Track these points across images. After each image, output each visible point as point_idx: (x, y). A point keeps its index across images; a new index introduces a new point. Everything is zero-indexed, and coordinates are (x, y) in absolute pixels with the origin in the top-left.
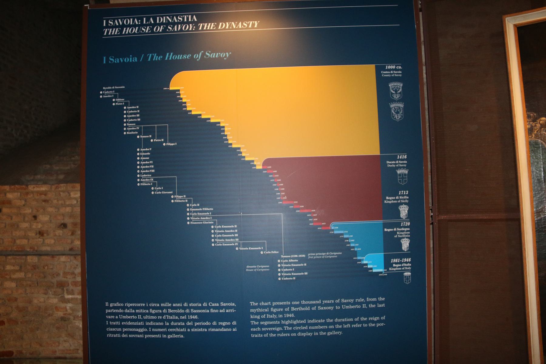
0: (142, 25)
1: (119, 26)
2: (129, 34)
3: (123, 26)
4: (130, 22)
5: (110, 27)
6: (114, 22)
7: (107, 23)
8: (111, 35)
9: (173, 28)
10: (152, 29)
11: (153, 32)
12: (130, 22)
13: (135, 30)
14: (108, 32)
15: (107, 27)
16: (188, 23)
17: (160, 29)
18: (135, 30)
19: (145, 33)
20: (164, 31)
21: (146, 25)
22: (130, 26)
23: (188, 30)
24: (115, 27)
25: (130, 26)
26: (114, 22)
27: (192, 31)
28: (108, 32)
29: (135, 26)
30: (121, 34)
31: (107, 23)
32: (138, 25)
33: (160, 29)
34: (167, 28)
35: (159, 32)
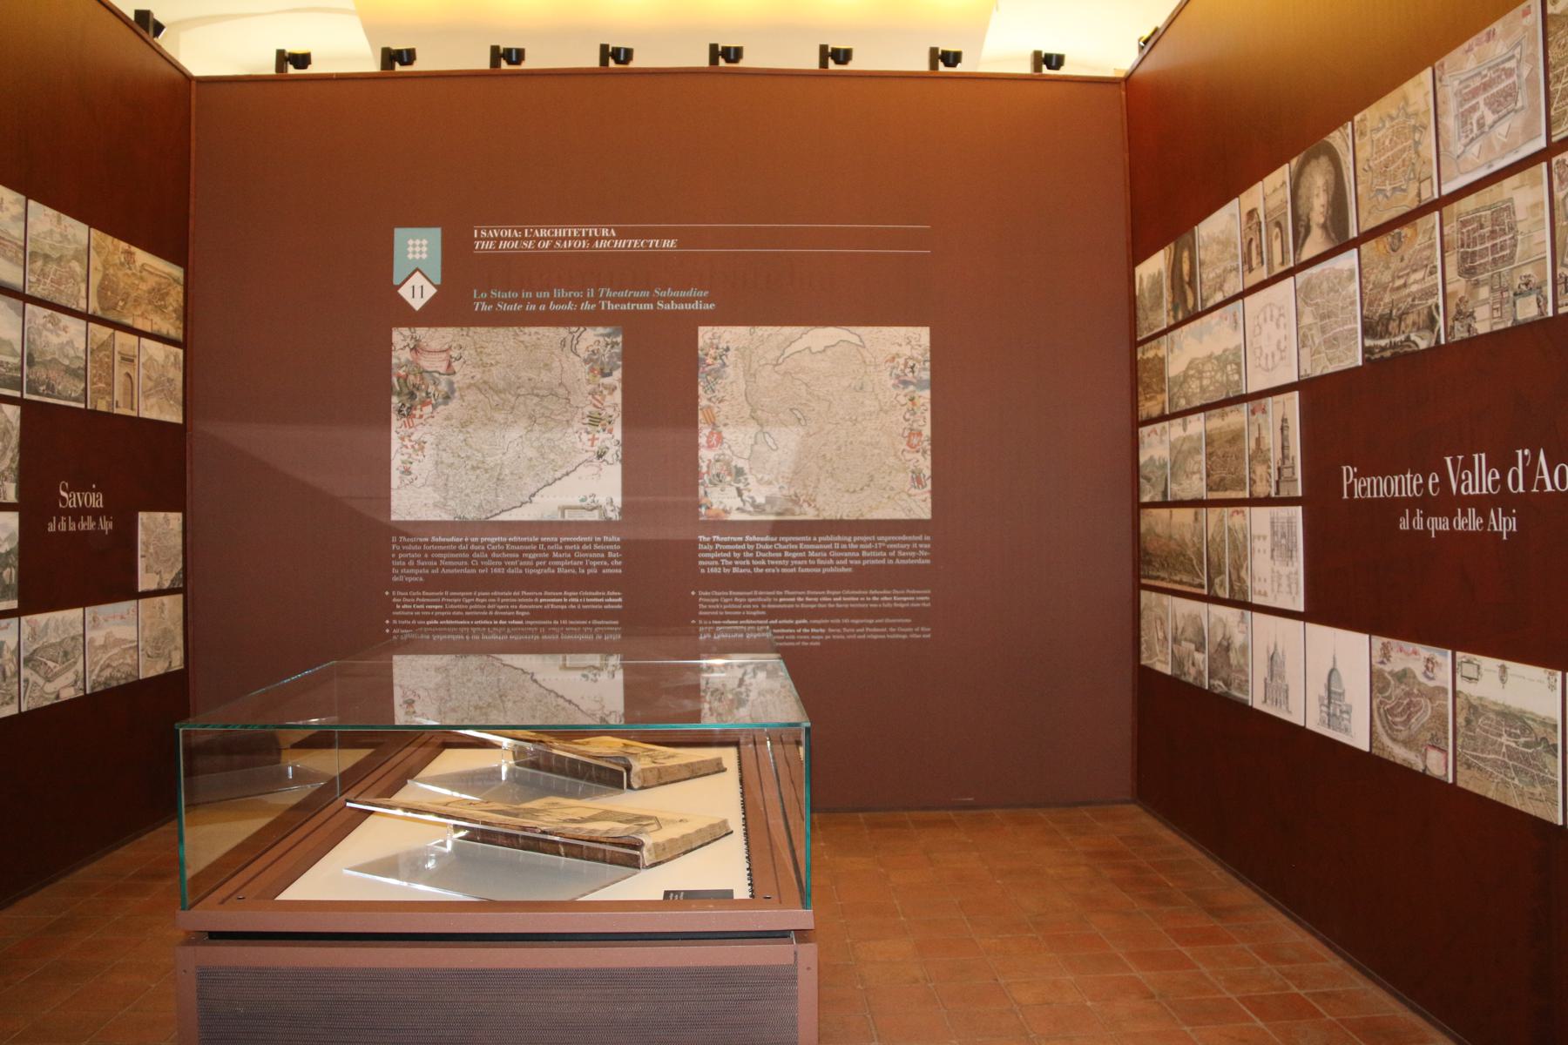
0: (523, 238)
1: (494, 239)
2: (506, 249)
3: (499, 239)
4: (508, 233)
5: (482, 239)
6: (487, 232)
7: (479, 234)
8: (484, 249)
9: (562, 243)
10: (536, 244)
11: (537, 248)
12: (508, 233)
13: (515, 245)
14: (480, 245)
15: (479, 239)
16: (581, 238)
17: (546, 244)
18: (515, 245)
19: (527, 249)
20: (551, 247)
21: (529, 239)
22: (507, 239)
23: (581, 248)
24: (489, 239)
25: (507, 239)
26: (487, 232)
27: (585, 249)
28: (480, 245)
29: (514, 239)
30: (497, 249)
31: (479, 234)
32: (517, 239)
33: (546, 244)
34: (554, 243)
35: (544, 249)
